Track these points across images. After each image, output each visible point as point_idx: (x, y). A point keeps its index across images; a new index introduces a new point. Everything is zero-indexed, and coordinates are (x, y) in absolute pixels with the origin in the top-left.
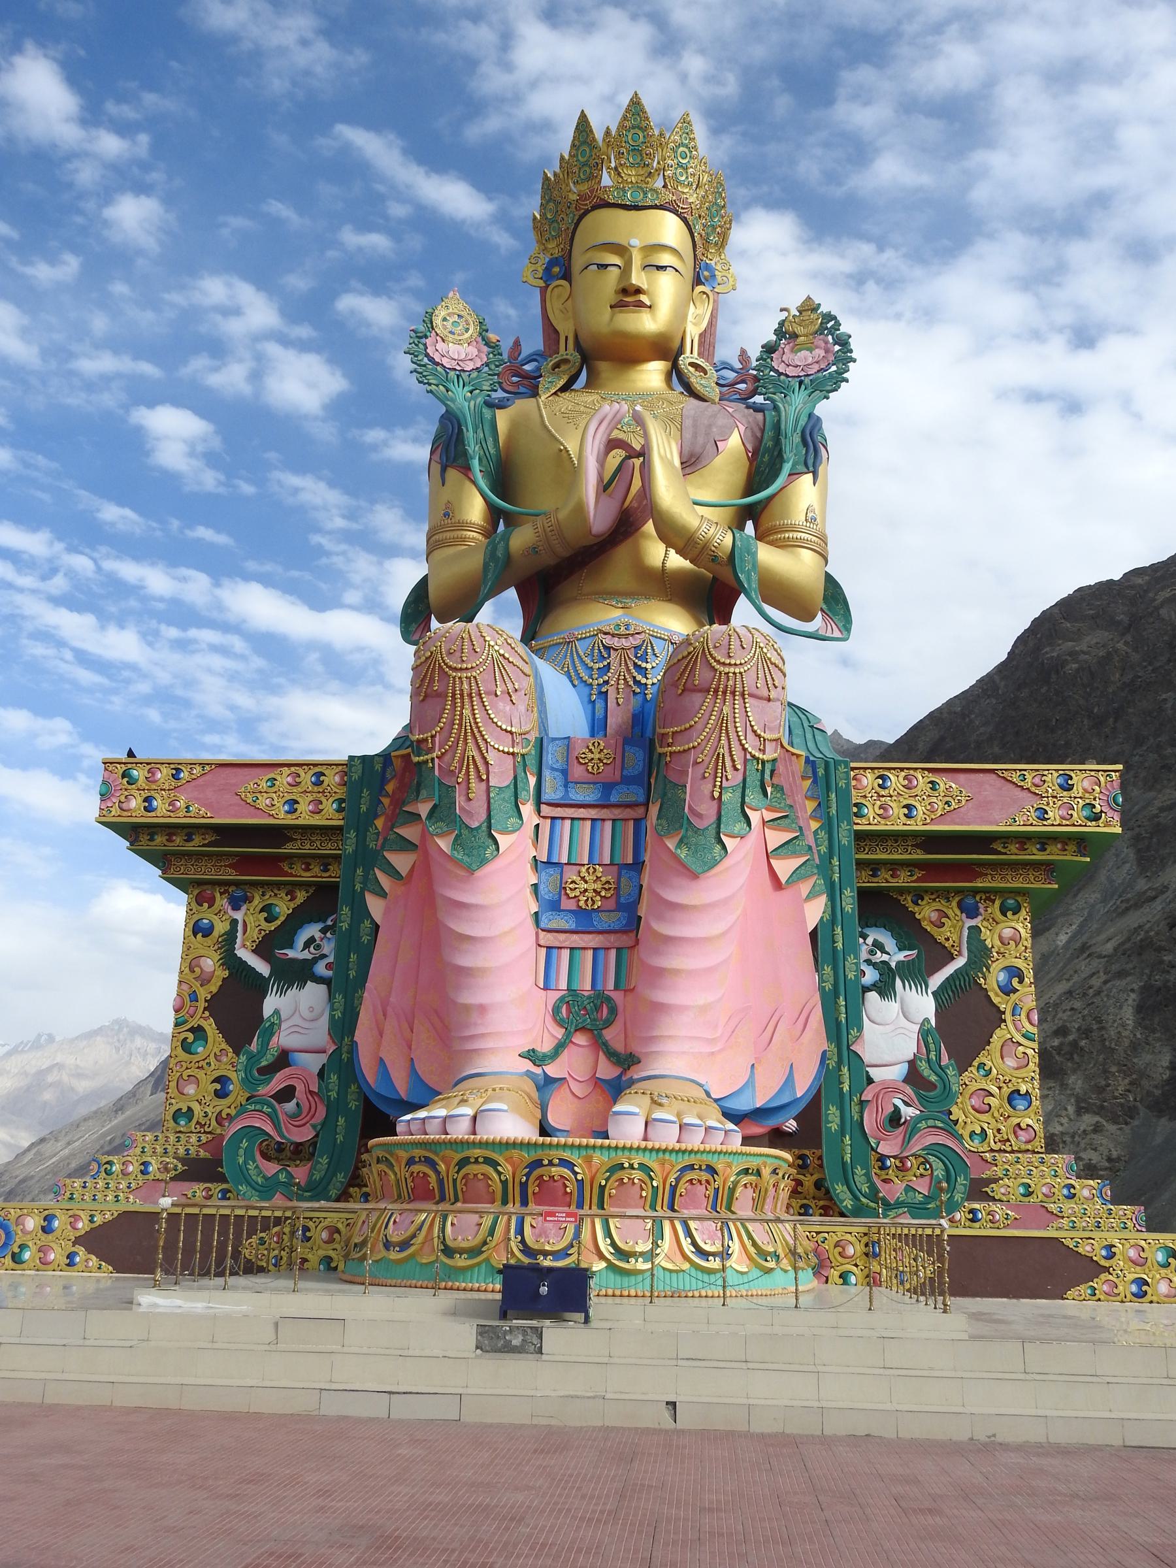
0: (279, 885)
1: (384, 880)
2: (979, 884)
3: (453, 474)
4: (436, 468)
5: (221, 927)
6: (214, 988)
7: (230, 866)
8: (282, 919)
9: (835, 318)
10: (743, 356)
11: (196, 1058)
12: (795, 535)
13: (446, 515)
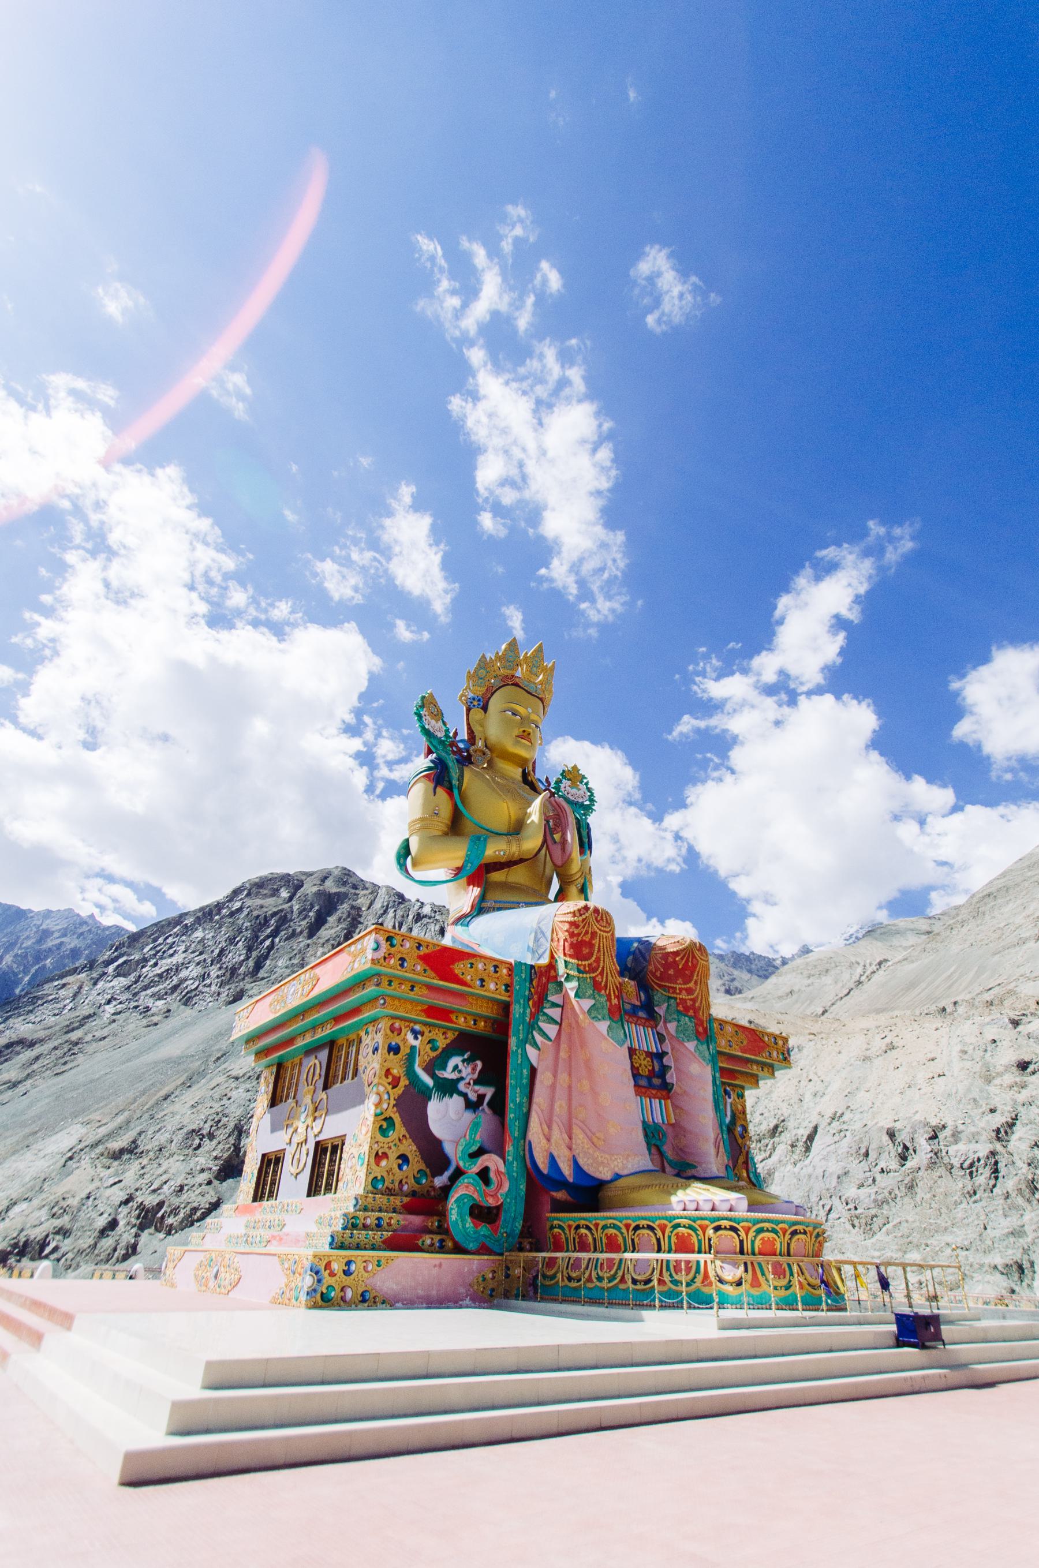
0: (440, 1027)
1: (538, 1038)
2: (737, 1082)
3: (439, 790)
4: (432, 785)
5: (404, 1051)
6: (399, 1090)
7: (422, 1011)
8: (440, 1050)
10: (547, 779)
11: (388, 1140)
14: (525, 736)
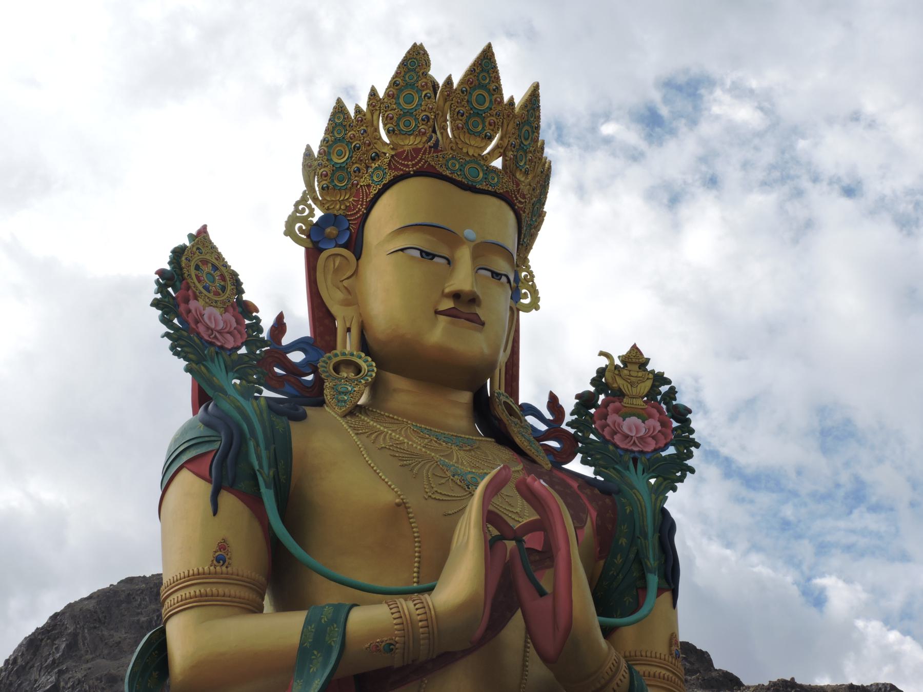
3: (228, 500)
9: (668, 381)
10: (553, 402)
12: (653, 670)
13: (220, 560)
14: (465, 307)
